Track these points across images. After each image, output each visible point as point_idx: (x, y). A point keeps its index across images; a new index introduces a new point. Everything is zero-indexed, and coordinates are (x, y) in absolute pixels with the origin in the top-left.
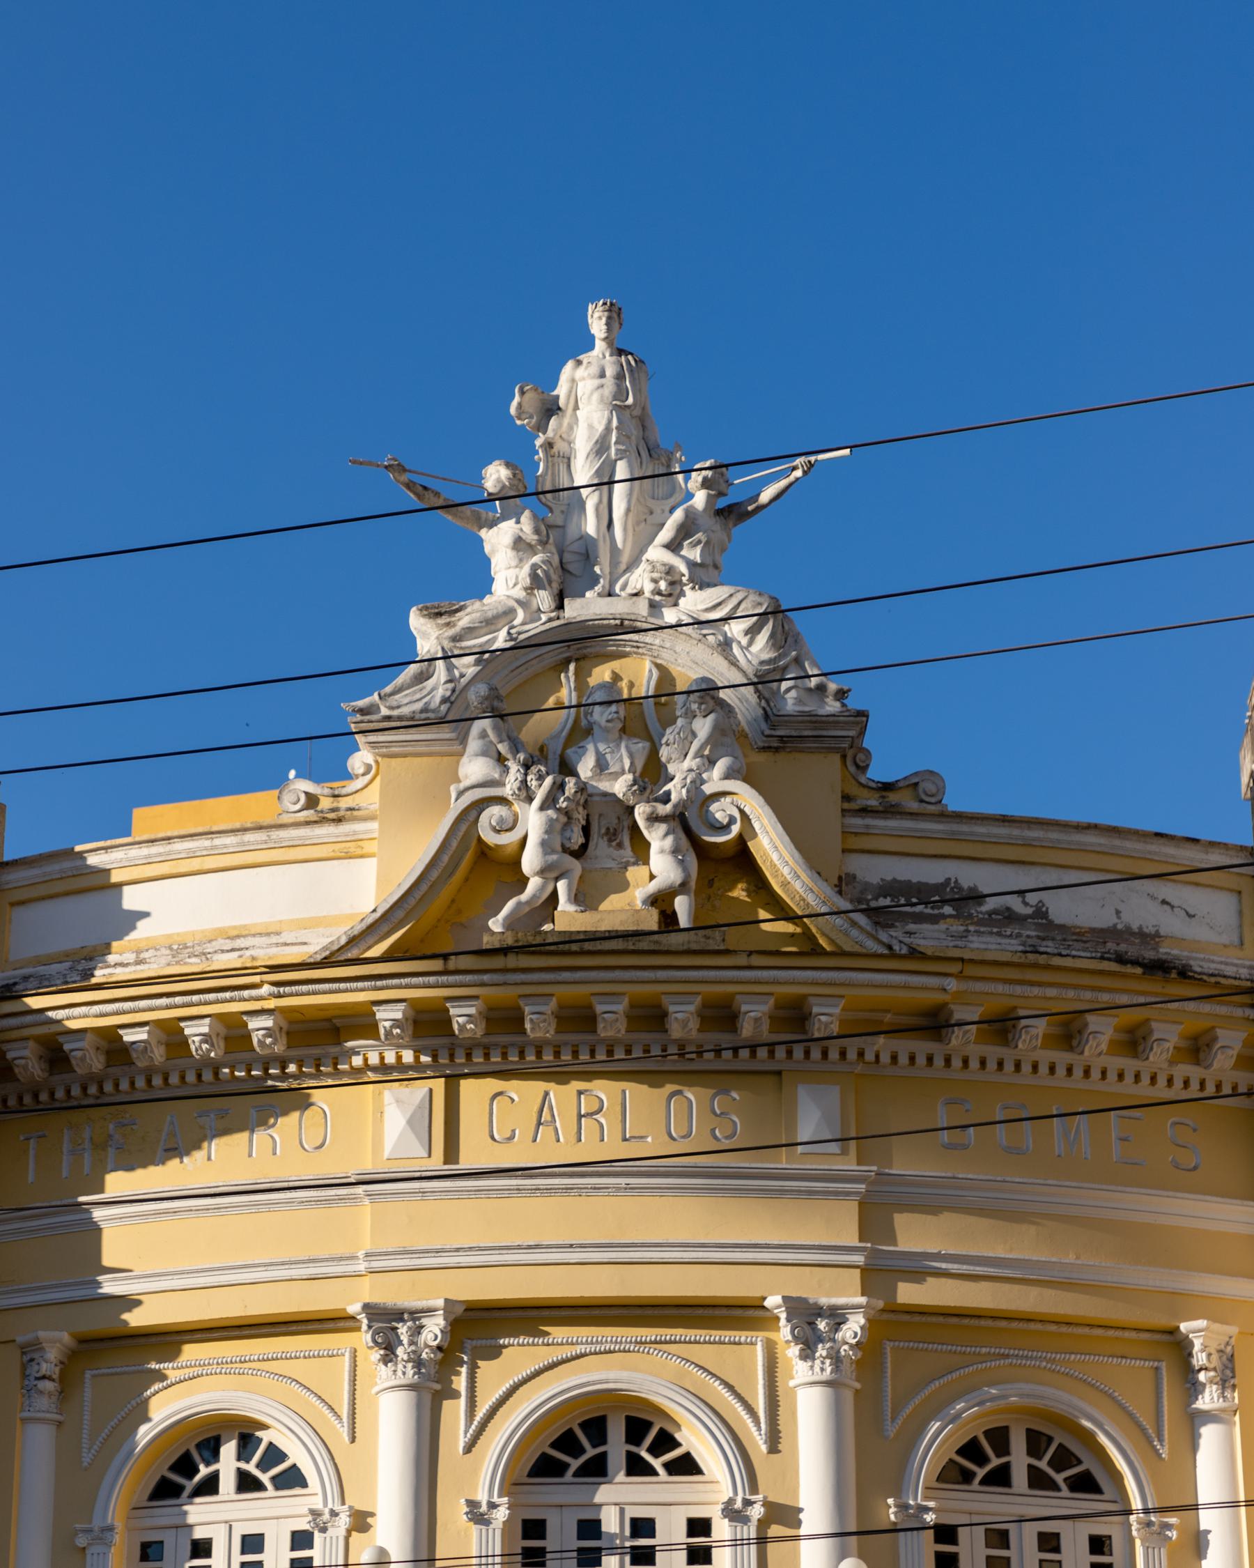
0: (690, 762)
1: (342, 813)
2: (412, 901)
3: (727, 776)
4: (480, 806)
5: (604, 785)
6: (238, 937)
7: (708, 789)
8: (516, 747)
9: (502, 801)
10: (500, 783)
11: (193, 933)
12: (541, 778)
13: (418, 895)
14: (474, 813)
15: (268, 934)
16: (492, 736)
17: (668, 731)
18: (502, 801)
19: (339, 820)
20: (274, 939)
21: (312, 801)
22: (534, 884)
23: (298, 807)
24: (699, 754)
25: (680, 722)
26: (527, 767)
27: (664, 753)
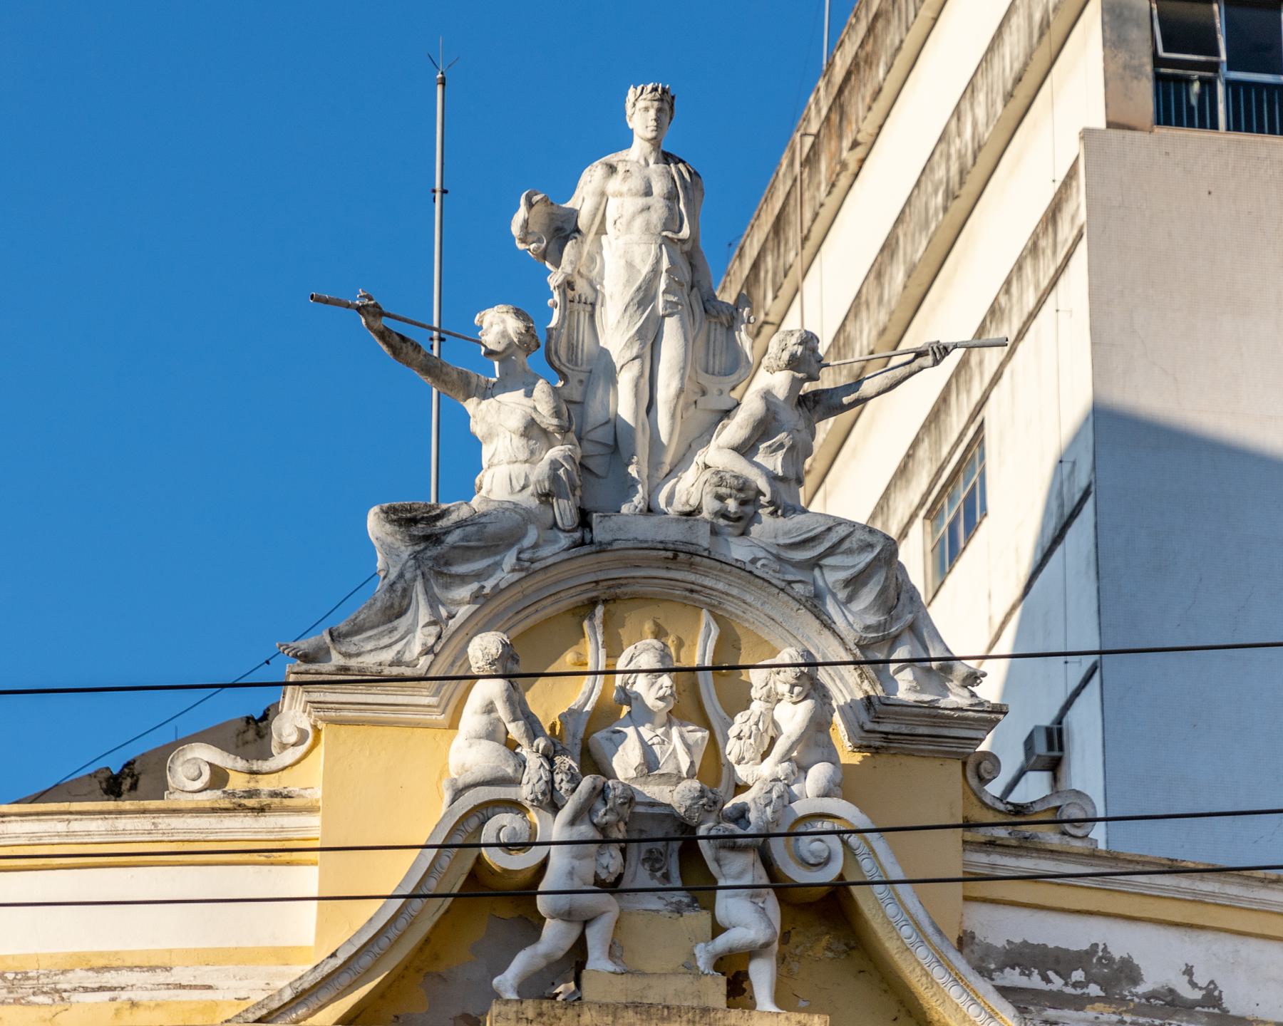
0: (770, 768)
1: (265, 800)
2: (384, 942)
3: (826, 794)
4: (485, 810)
5: (654, 791)
6: (107, 968)
7: (800, 808)
8: (533, 728)
9: (515, 806)
10: (514, 782)
11: (37, 958)
12: (574, 781)
13: (393, 933)
14: (474, 822)
15: (152, 969)
16: (502, 711)
17: (739, 718)
18: (515, 806)
19: (261, 810)
20: (161, 977)
21: (219, 778)
22: (552, 929)
23: (199, 784)
24: (786, 758)
25: (757, 707)
26: (549, 757)
27: (732, 749)
